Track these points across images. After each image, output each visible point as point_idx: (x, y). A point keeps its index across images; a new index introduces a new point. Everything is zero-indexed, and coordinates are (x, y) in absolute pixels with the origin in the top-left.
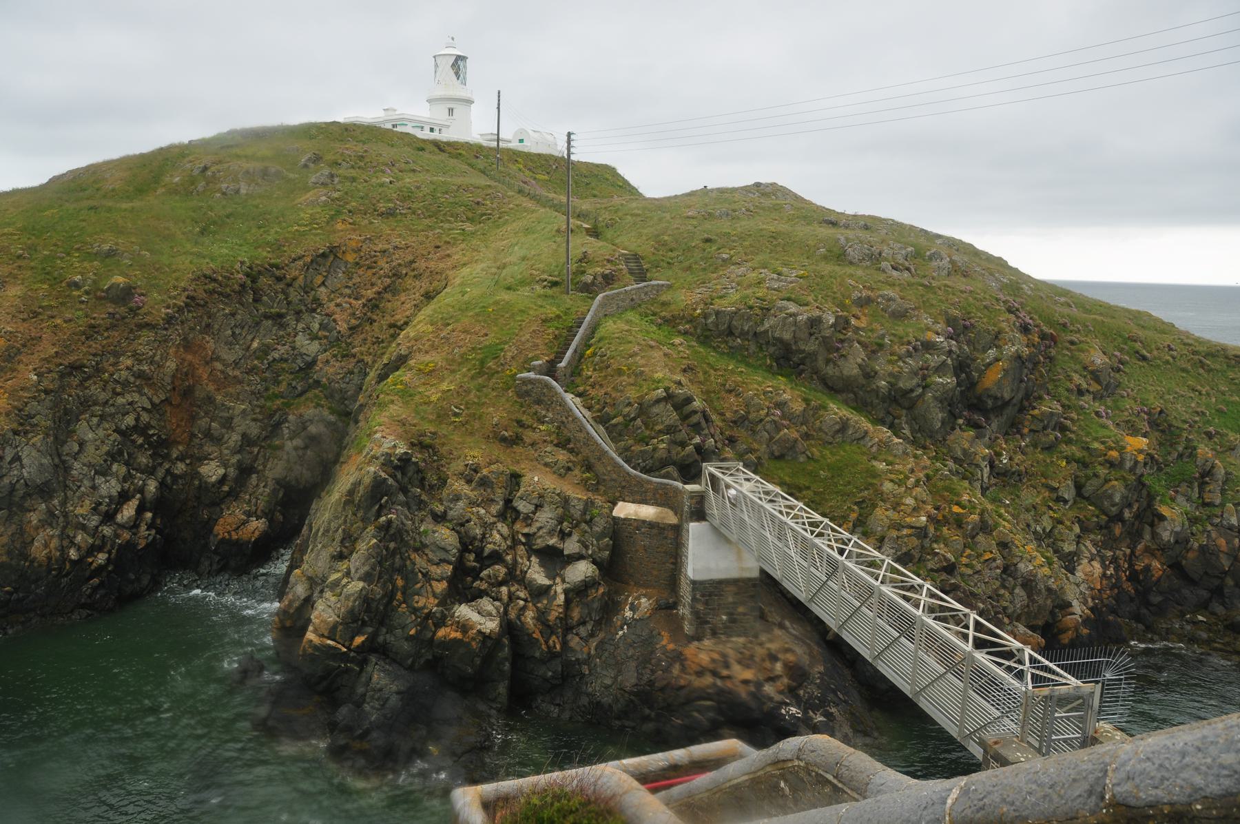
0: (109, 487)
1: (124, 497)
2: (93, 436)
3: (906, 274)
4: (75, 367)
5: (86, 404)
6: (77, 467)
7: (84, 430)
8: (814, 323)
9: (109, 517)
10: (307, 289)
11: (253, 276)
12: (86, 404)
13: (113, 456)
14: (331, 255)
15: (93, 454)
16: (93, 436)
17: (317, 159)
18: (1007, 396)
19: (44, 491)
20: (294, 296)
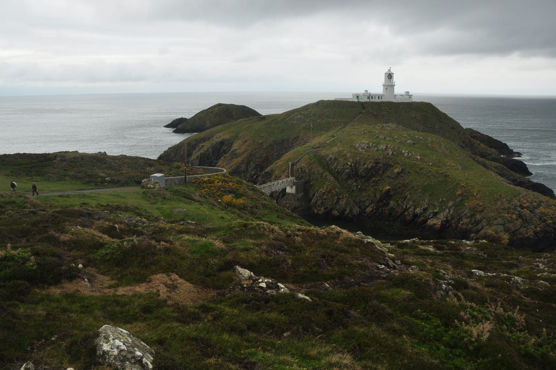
0: (253, 173)
1: (255, 174)
2: (252, 165)
3: (364, 150)
4: (252, 155)
5: (252, 160)
6: (249, 169)
7: (251, 164)
8: (331, 159)
9: (252, 177)
10: (292, 143)
11: (283, 141)
12: (252, 160)
13: (254, 168)
14: (297, 138)
15: (252, 167)
16: (252, 165)
17: (315, 114)
18: (364, 175)
19: (244, 172)
20: (289, 144)
